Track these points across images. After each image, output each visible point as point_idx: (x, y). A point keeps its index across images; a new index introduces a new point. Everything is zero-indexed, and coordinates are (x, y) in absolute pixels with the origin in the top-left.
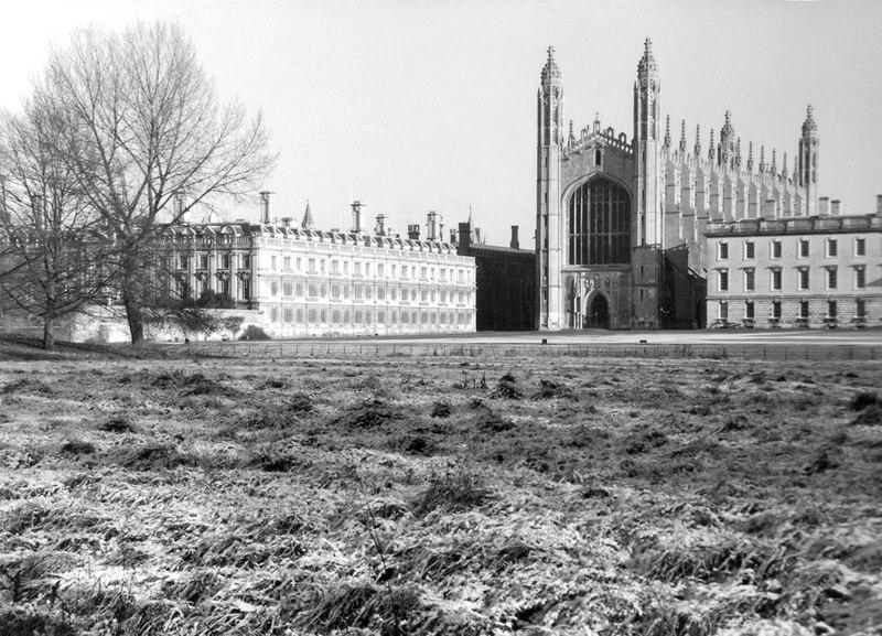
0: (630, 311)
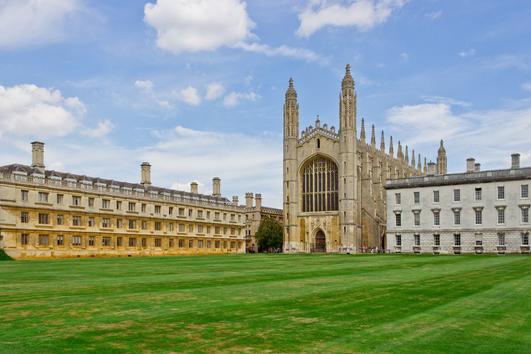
0: (338, 241)
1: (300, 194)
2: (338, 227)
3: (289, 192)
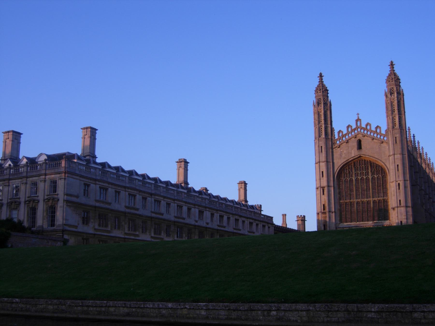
3: (325, 199)
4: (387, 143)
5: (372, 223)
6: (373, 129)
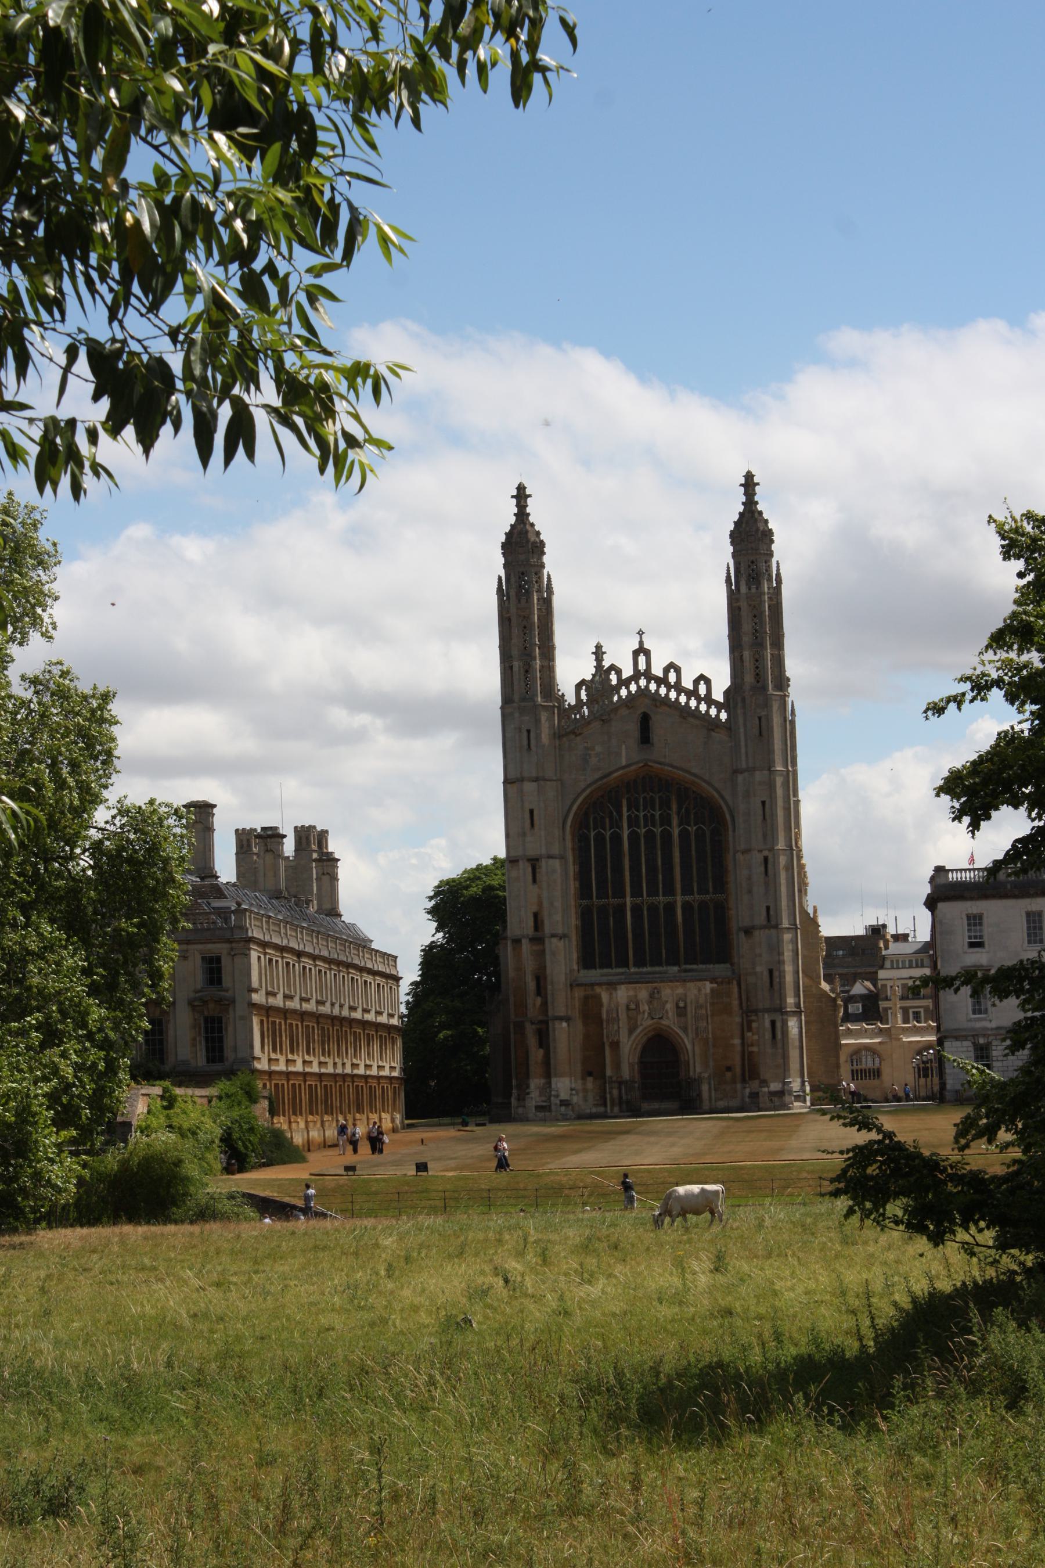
0: (738, 1070)
1: (573, 903)
2: (738, 1019)
3: (539, 897)
4: (729, 729)
5: (679, 971)
6: (687, 683)
